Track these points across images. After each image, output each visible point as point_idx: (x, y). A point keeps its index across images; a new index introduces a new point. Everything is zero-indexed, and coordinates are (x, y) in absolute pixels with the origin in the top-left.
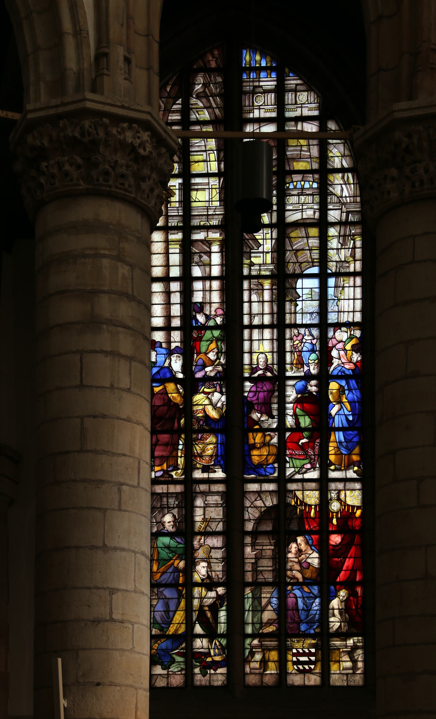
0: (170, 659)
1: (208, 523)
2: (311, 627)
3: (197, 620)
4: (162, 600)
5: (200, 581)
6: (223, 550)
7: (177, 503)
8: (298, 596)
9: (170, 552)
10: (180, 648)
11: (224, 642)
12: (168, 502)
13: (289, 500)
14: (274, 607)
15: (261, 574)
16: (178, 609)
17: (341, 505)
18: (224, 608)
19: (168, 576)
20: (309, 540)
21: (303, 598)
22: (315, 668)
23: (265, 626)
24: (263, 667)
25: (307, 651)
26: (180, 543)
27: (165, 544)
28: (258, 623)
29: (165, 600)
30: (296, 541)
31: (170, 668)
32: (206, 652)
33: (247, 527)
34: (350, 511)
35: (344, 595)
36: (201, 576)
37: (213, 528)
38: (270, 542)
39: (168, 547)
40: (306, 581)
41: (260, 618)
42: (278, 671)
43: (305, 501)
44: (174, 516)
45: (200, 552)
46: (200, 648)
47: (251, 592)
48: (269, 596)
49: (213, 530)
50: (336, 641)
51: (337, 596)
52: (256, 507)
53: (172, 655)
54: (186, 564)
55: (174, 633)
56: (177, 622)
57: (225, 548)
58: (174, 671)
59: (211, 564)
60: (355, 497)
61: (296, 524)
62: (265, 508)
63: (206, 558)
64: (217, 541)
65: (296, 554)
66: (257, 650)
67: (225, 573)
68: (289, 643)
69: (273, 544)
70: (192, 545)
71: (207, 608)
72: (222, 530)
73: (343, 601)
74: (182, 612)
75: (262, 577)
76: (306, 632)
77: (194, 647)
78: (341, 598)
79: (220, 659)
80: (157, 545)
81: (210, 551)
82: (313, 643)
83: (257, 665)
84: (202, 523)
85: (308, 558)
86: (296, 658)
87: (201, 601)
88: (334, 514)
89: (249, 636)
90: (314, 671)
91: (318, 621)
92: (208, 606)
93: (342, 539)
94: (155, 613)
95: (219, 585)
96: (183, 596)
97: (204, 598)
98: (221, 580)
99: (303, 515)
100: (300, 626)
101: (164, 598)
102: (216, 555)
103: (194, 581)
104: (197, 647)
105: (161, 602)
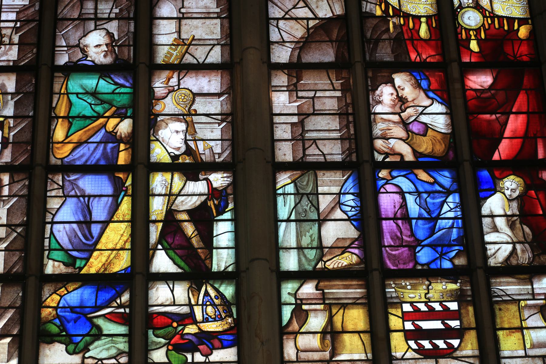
0: (88, 330)
1: (188, 49)
2: (442, 256)
3: (159, 242)
4: (74, 200)
5: (167, 159)
6: (222, 99)
7: (117, 11)
8: (405, 190)
9: (99, 102)
10: (115, 305)
11: (228, 291)
12: (96, 8)
13: (368, 7)
14: (350, 214)
15: (314, 145)
16: (112, 217)
17: (484, 17)
18: (227, 215)
19: (92, 149)
20: (421, 80)
21: (418, 193)
22: (463, 344)
23: (331, 254)
24: (330, 344)
25: (437, 307)
26: (122, 86)
27: (87, 86)
28: (312, 248)
29: (81, 199)
30: (392, 82)
31: (89, 350)
32: (182, 312)
33: (277, 55)
34: (506, 28)
35: (514, 186)
36: (170, 150)
37: (200, 58)
38: (332, 84)
39: (94, 94)
40: (420, 160)
41: (316, 236)
42: (370, 356)
43: (404, 9)
44: (110, 34)
45: (168, 102)
46: (167, 303)
47: (293, 182)
48: (335, 189)
49: (200, 60)
50: (508, 284)
51: (498, 189)
52: (296, 19)
53: (95, 320)
54: (135, 126)
55: (103, 270)
56: (110, 246)
57: (226, 96)
58: (99, 357)
59: (196, 125)
60: (513, 3)
61: (389, 50)
62: (317, 21)
63: (183, 115)
64: (209, 81)
65: (394, 106)
66: (313, 307)
67: (227, 143)
68: (393, 290)
69: (340, 88)
70: (151, 90)
71: (184, 217)
72: (220, 60)
73: (513, 200)
74: (123, 226)
75: (317, 152)
76: (433, 266)
77: (151, 302)
78: (508, 193)
79: (220, 329)
80: (66, 88)
81: (193, 101)
82: (451, 291)
83: (315, 341)
84: (174, 47)
85: (421, 113)
86: (413, 324)
87: (171, 201)
88: (471, 33)
89: (290, 276)
90: (458, 353)
91: (459, 241)
92: (188, 212)
93: (495, 80)
94: (56, 227)
95: (214, 167)
96: (126, 191)
97: (179, 195)
98: (219, 158)
99: (402, 33)
100: (415, 253)
101: (79, 194)
102: (207, 109)
103: (153, 160)
104: (159, 302)
105: (71, 203)
